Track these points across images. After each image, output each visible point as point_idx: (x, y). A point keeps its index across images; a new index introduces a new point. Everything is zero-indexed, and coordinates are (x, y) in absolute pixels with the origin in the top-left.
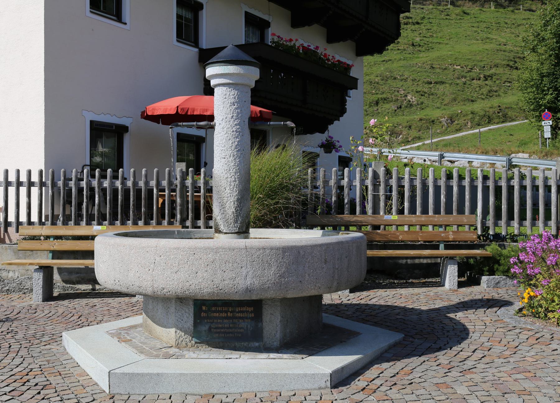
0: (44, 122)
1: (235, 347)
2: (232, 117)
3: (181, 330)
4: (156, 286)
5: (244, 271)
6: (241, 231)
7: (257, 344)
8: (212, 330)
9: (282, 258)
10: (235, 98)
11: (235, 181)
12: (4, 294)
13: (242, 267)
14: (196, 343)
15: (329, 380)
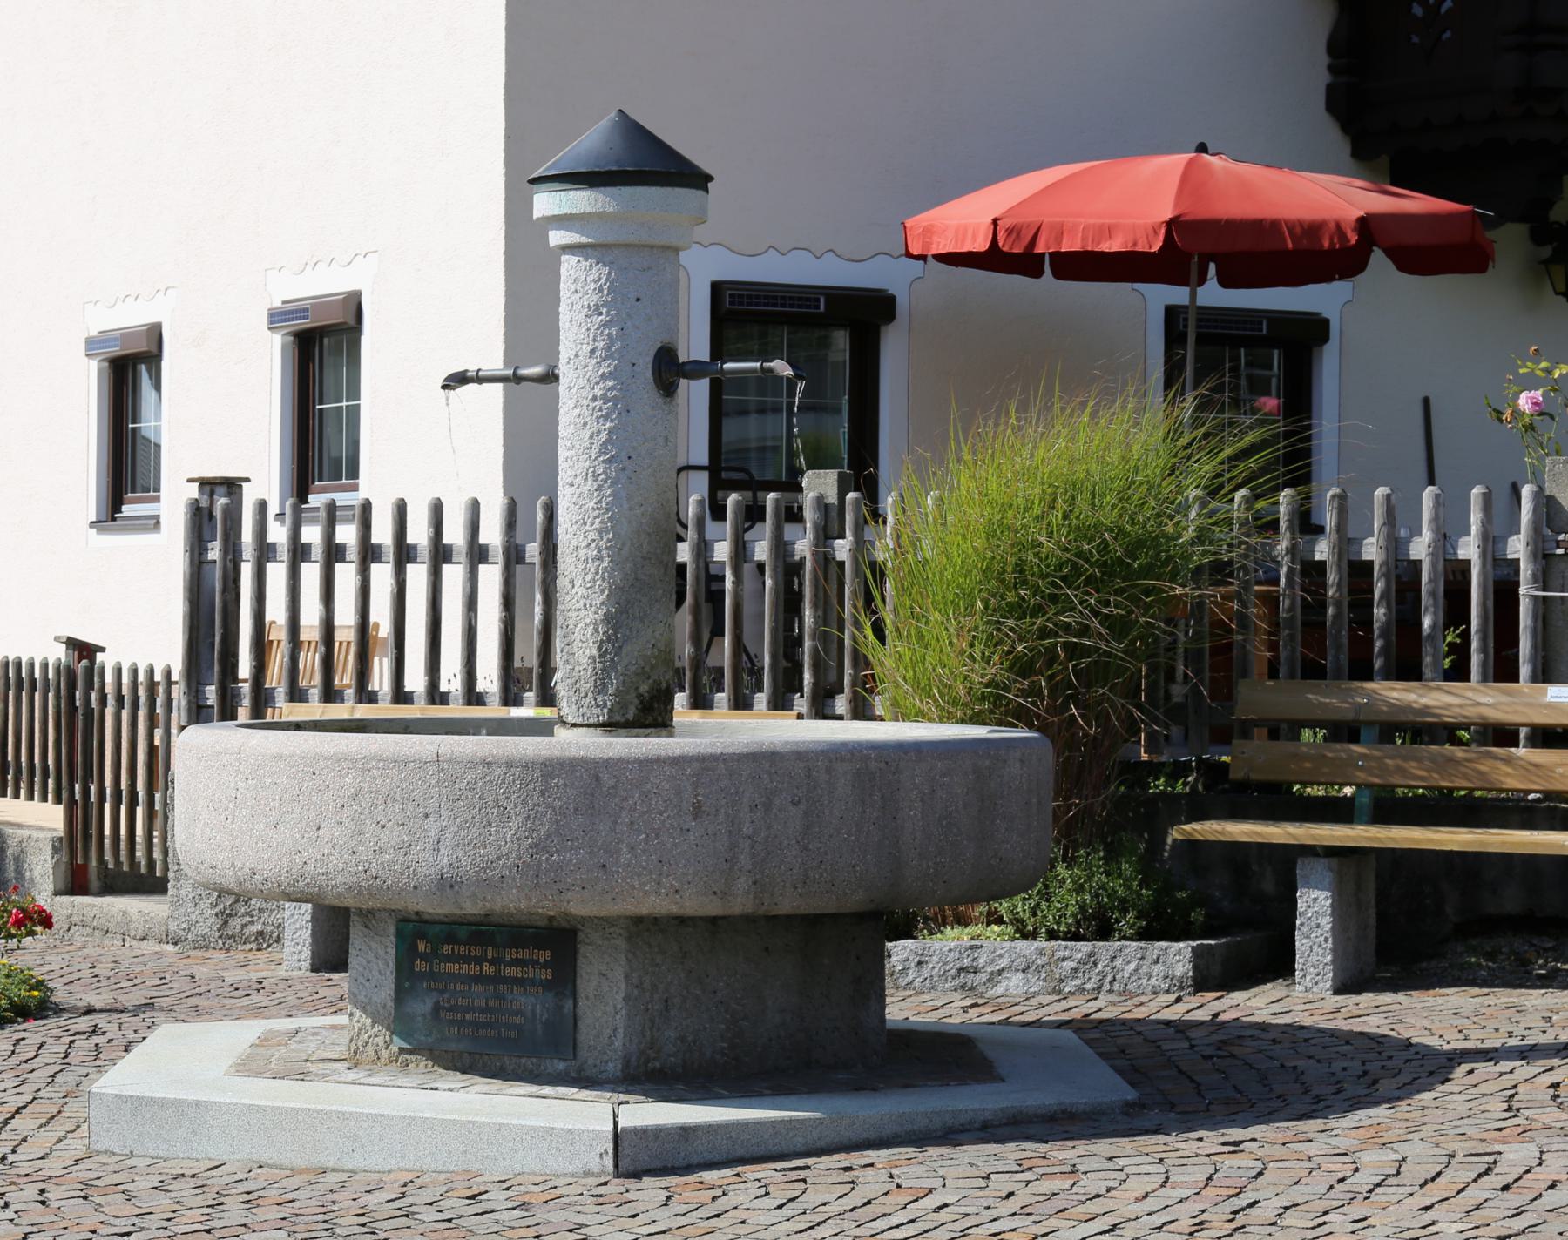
0: (502, 302)
1: (502, 1069)
2: (593, 351)
3: (364, 1010)
4: (238, 864)
5: (432, 827)
6: (617, 718)
7: (561, 1066)
8: (442, 1013)
9: (543, 793)
10: (601, 290)
11: (600, 558)
12: (248, 946)
13: (426, 816)
14: (402, 1050)
15: (610, 1152)
